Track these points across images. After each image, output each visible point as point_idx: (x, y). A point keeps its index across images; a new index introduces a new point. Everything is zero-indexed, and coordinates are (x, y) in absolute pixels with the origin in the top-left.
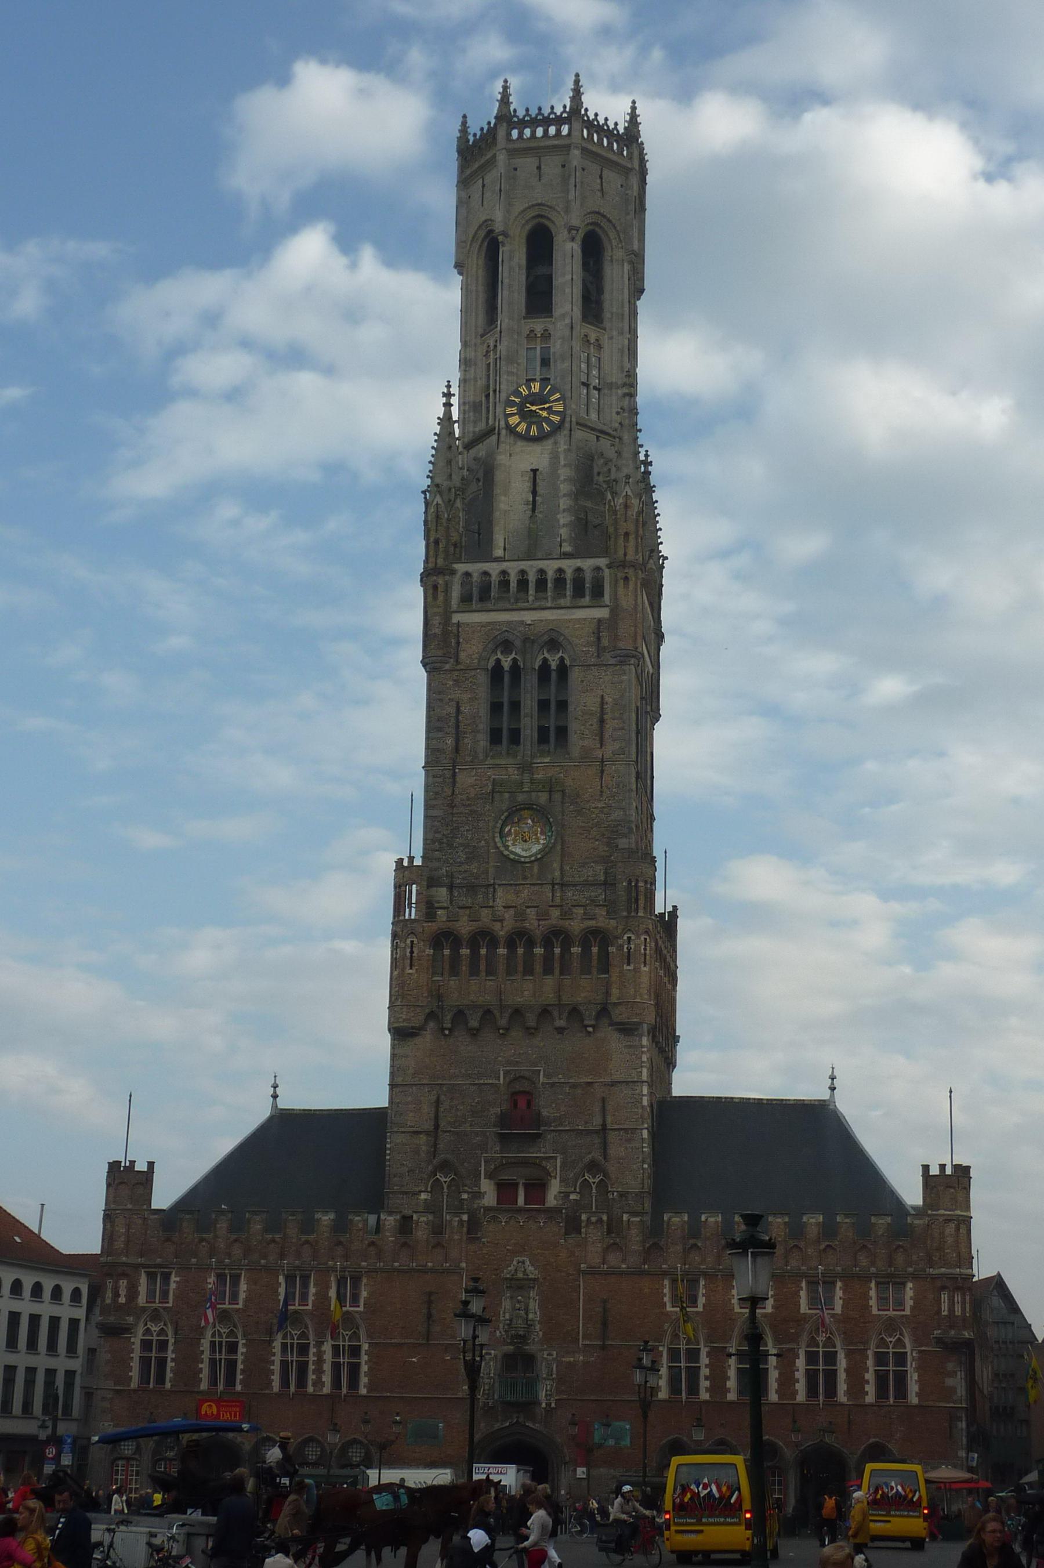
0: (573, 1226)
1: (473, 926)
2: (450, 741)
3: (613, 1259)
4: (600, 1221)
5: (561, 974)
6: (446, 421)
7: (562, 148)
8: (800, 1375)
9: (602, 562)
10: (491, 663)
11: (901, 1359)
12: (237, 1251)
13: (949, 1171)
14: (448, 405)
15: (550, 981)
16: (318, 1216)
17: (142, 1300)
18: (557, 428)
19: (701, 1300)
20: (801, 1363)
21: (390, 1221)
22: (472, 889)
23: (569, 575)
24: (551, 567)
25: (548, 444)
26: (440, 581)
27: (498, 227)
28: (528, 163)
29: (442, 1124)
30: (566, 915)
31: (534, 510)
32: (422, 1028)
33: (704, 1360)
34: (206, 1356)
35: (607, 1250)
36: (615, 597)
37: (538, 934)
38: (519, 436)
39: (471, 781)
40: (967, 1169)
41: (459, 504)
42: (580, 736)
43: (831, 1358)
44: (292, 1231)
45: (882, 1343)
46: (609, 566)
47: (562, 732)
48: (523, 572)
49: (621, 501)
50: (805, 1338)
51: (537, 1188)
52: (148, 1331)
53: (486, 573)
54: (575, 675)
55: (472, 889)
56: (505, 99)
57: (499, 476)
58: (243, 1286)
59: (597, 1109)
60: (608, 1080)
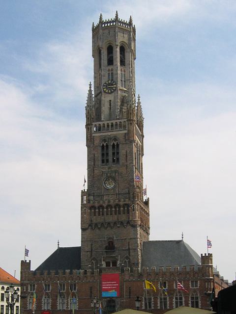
0: (123, 271)
1: (99, 205)
2: (93, 163)
3: (131, 278)
5: (119, 214)
6: (90, 91)
7: (114, 27)
8: (174, 303)
9: (126, 120)
10: (102, 145)
11: (197, 298)
12: (49, 279)
13: (207, 255)
14: (90, 87)
15: (116, 216)
16: (66, 271)
17: (29, 291)
18: (115, 90)
20: (174, 300)
21: (82, 271)
22: (98, 196)
23: (118, 123)
24: (114, 122)
25: (113, 94)
26: (89, 127)
27: (100, 46)
28: (107, 31)
30: (119, 201)
31: (110, 109)
32: (88, 228)
33: (153, 300)
34: (43, 302)
35: (130, 276)
36: (128, 128)
37: (113, 206)
38: (106, 93)
40: (211, 254)
41: (93, 109)
42: (122, 160)
43: (181, 299)
45: (193, 295)
47: (118, 159)
48: (108, 123)
49: (129, 106)
50: (175, 294)
51: (115, 264)
53: (100, 124)
54: (120, 146)
55: (98, 196)
56: (101, 18)
57: (102, 102)
58: (51, 287)
59: (127, 245)
60: (130, 238)
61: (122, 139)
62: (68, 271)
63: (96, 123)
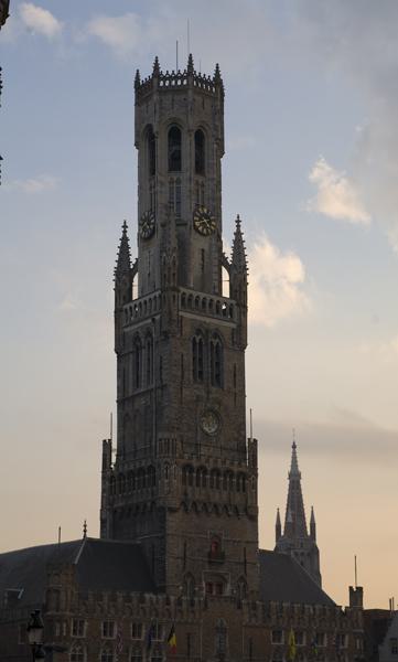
2: (179, 373)
4: (248, 604)
9: (234, 302)
12: (112, 611)
17: (71, 635)
19: (283, 640)
28: (199, 99)
29: (188, 553)
30: (232, 464)
37: (222, 470)
38: (199, 232)
39: (188, 393)
42: (227, 378)
44: (135, 601)
46: (237, 305)
47: (218, 376)
51: (220, 586)
52: (74, 650)
54: (225, 352)
58: (115, 628)
61: (227, 337)
62: (147, 596)
63: (188, 292)
